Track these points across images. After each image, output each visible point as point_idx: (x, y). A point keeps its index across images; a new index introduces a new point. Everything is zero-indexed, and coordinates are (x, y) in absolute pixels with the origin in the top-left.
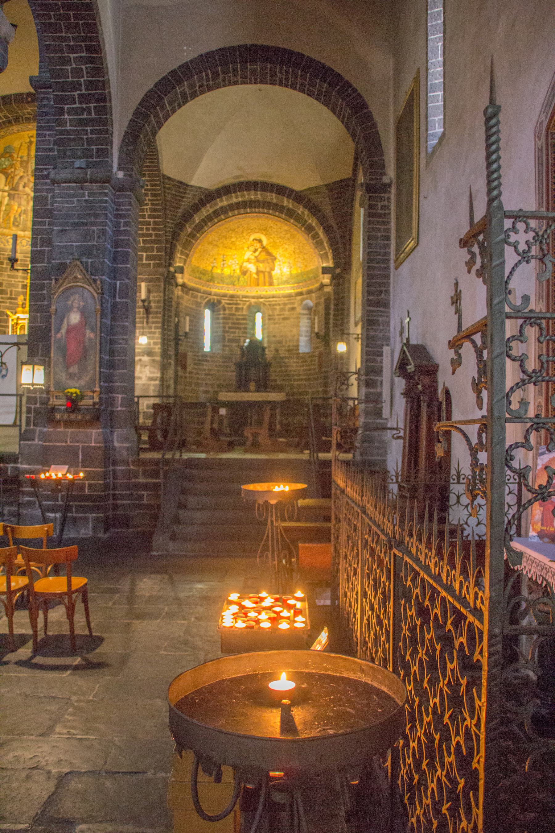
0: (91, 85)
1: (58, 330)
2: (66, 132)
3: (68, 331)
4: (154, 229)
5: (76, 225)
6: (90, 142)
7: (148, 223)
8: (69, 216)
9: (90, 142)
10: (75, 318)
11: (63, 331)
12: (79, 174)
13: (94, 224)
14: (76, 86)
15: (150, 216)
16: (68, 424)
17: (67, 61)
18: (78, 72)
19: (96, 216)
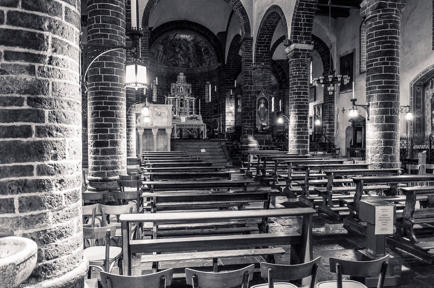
0: (267, 43)
1: (258, 109)
2: (259, 55)
3: (261, 109)
4: (232, 72)
5: (261, 80)
6: (264, 58)
7: (231, 70)
8: (260, 78)
9: (264, 58)
10: (262, 105)
11: (259, 109)
12: (262, 67)
13: (266, 80)
14: (264, 43)
15: (232, 67)
16: (261, 133)
17: (263, 37)
18: (265, 40)
19: (267, 78)
